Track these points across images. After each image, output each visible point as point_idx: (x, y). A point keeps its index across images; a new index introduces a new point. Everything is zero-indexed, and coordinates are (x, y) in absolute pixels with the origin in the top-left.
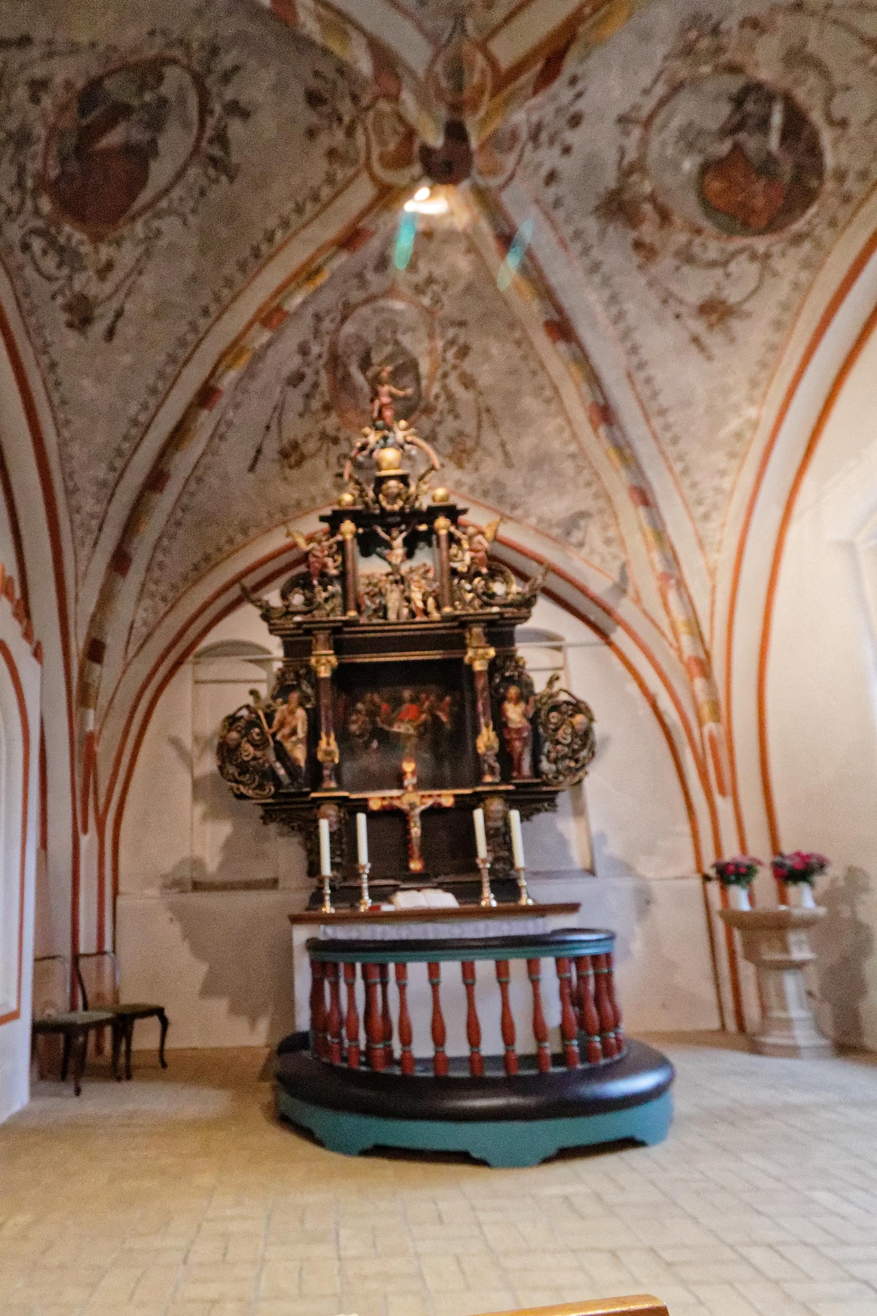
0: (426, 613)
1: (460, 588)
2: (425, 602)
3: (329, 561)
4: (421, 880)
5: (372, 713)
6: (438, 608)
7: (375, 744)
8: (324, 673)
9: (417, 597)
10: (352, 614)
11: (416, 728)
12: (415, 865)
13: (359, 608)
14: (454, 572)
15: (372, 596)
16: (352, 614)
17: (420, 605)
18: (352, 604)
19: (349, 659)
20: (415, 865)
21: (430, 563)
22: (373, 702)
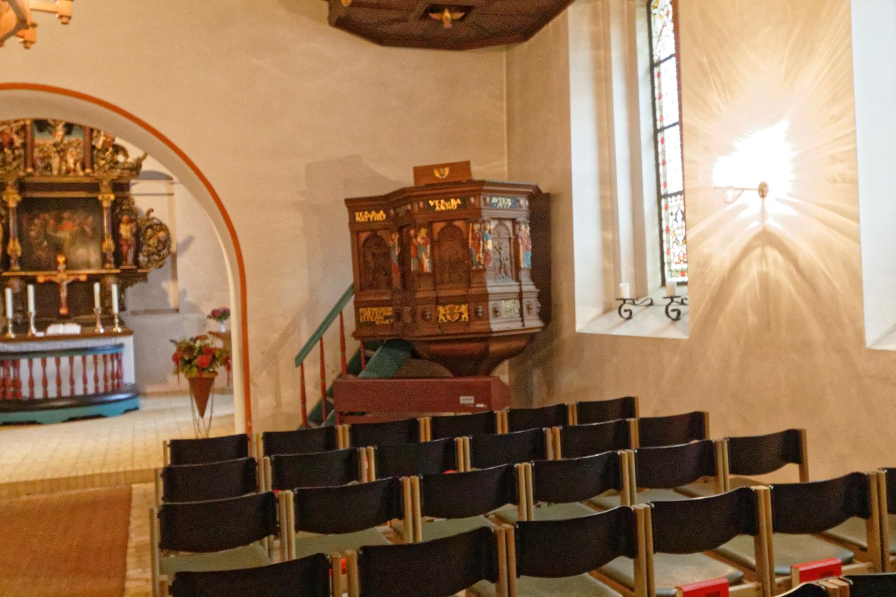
0: (75, 170)
1: (98, 157)
2: (75, 164)
3: (15, 137)
4: (64, 319)
5: (45, 226)
6: (83, 168)
7: (45, 243)
8: (12, 204)
9: (71, 161)
10: (30, 170)
11: (71, 234)
12: (63, 311)
13: (34, 166)
14: (93, 147)
15: (43, 159)
16: (30, 170)
17: (72, 166)
18: (29, 163)
19: (29, 194)
20: (63, 311)
21: (81, 139)
22: (45, 220)
